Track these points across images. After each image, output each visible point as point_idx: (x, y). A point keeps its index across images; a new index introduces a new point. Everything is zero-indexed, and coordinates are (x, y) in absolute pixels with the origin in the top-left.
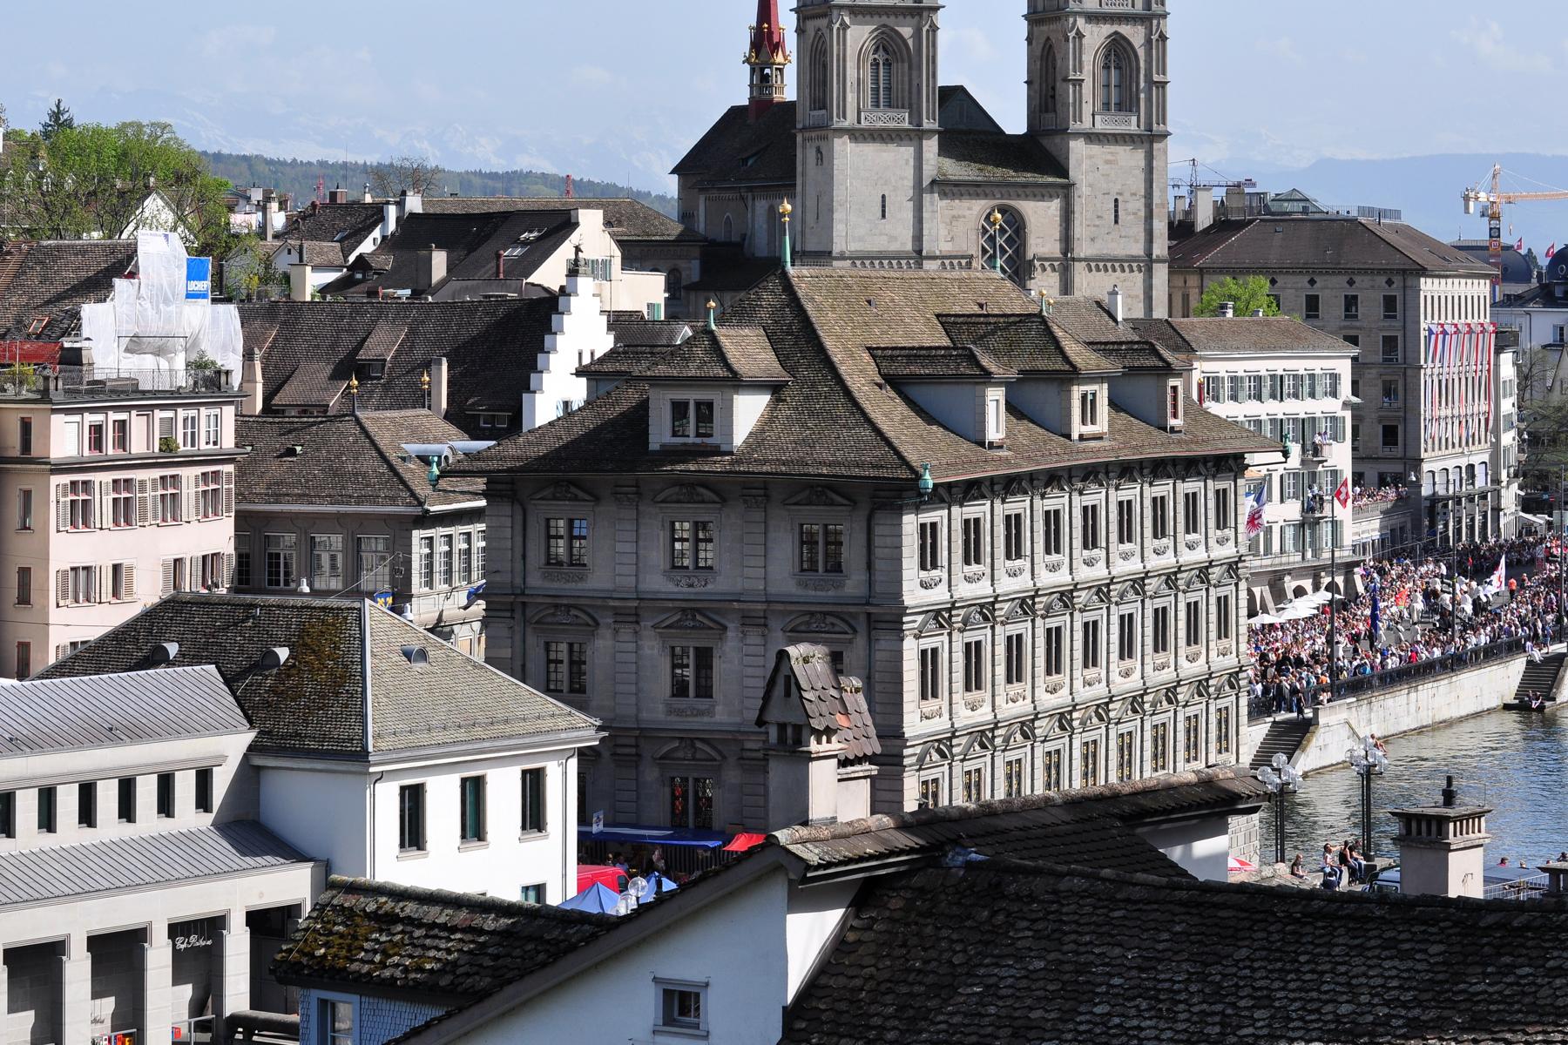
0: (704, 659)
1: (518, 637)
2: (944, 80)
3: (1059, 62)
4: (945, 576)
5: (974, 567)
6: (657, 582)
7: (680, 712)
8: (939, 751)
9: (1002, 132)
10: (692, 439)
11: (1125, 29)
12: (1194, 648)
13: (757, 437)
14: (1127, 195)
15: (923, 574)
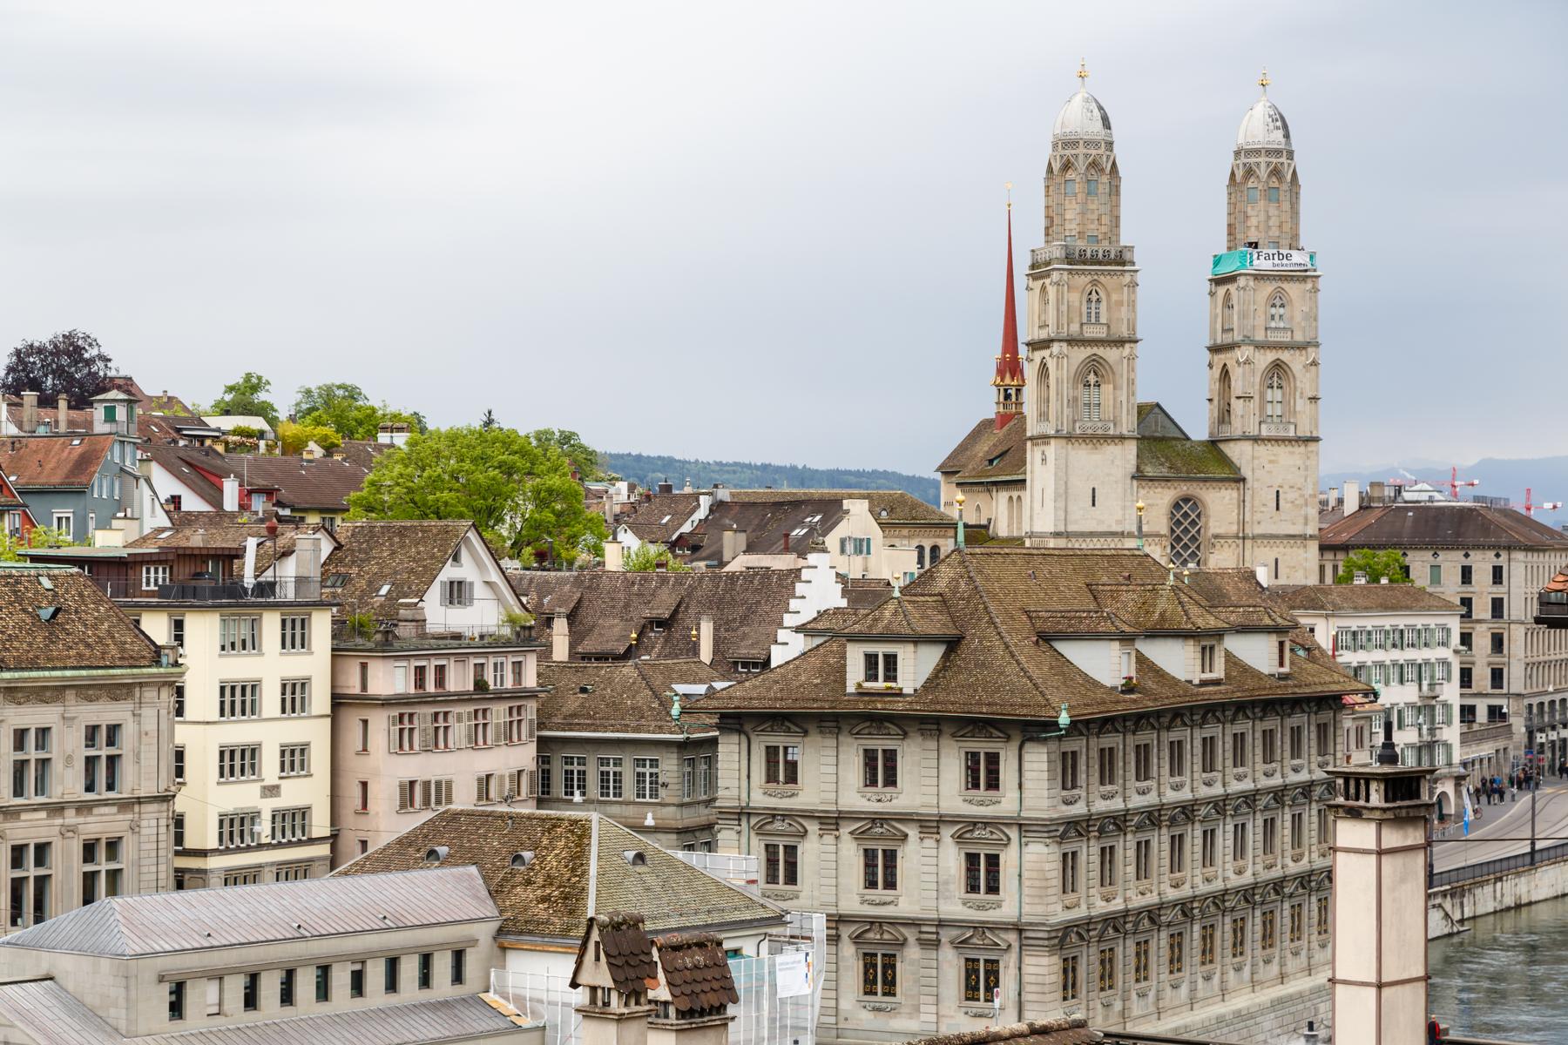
0: (890, 857)
1: (744, 840)
2: (1144, 397)
3: (1233, 383)
4: (1084, 794)
5: (1109, 788)
6: (854, 796)
7: (872, 903)
8: (1078, 933)
9: (1188, 439)
10: (880, 684)
11: (1285, 356)
12: (1298, 851)
13: (932, 683)
14: (1286, 488)
15: (1065, 793)
